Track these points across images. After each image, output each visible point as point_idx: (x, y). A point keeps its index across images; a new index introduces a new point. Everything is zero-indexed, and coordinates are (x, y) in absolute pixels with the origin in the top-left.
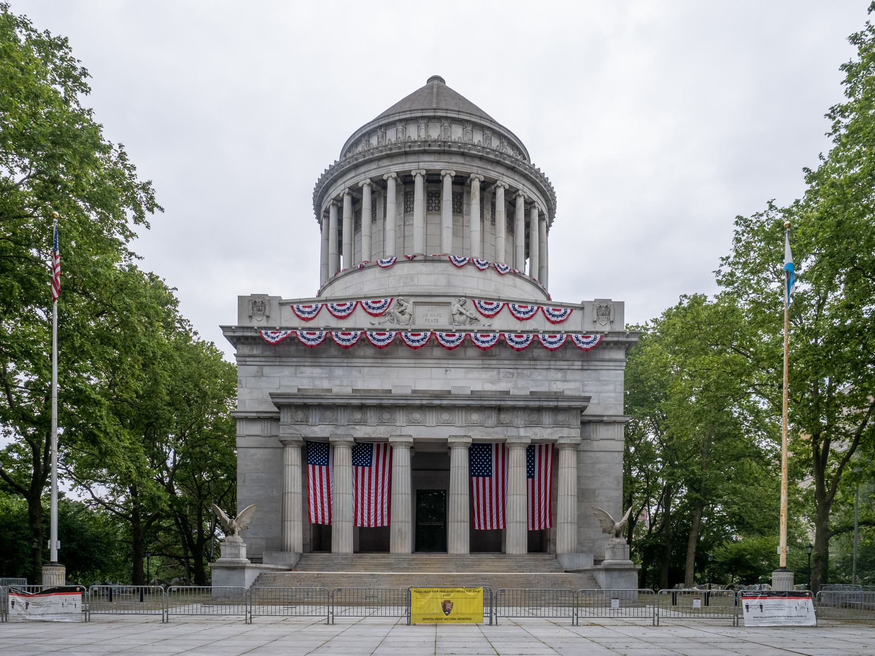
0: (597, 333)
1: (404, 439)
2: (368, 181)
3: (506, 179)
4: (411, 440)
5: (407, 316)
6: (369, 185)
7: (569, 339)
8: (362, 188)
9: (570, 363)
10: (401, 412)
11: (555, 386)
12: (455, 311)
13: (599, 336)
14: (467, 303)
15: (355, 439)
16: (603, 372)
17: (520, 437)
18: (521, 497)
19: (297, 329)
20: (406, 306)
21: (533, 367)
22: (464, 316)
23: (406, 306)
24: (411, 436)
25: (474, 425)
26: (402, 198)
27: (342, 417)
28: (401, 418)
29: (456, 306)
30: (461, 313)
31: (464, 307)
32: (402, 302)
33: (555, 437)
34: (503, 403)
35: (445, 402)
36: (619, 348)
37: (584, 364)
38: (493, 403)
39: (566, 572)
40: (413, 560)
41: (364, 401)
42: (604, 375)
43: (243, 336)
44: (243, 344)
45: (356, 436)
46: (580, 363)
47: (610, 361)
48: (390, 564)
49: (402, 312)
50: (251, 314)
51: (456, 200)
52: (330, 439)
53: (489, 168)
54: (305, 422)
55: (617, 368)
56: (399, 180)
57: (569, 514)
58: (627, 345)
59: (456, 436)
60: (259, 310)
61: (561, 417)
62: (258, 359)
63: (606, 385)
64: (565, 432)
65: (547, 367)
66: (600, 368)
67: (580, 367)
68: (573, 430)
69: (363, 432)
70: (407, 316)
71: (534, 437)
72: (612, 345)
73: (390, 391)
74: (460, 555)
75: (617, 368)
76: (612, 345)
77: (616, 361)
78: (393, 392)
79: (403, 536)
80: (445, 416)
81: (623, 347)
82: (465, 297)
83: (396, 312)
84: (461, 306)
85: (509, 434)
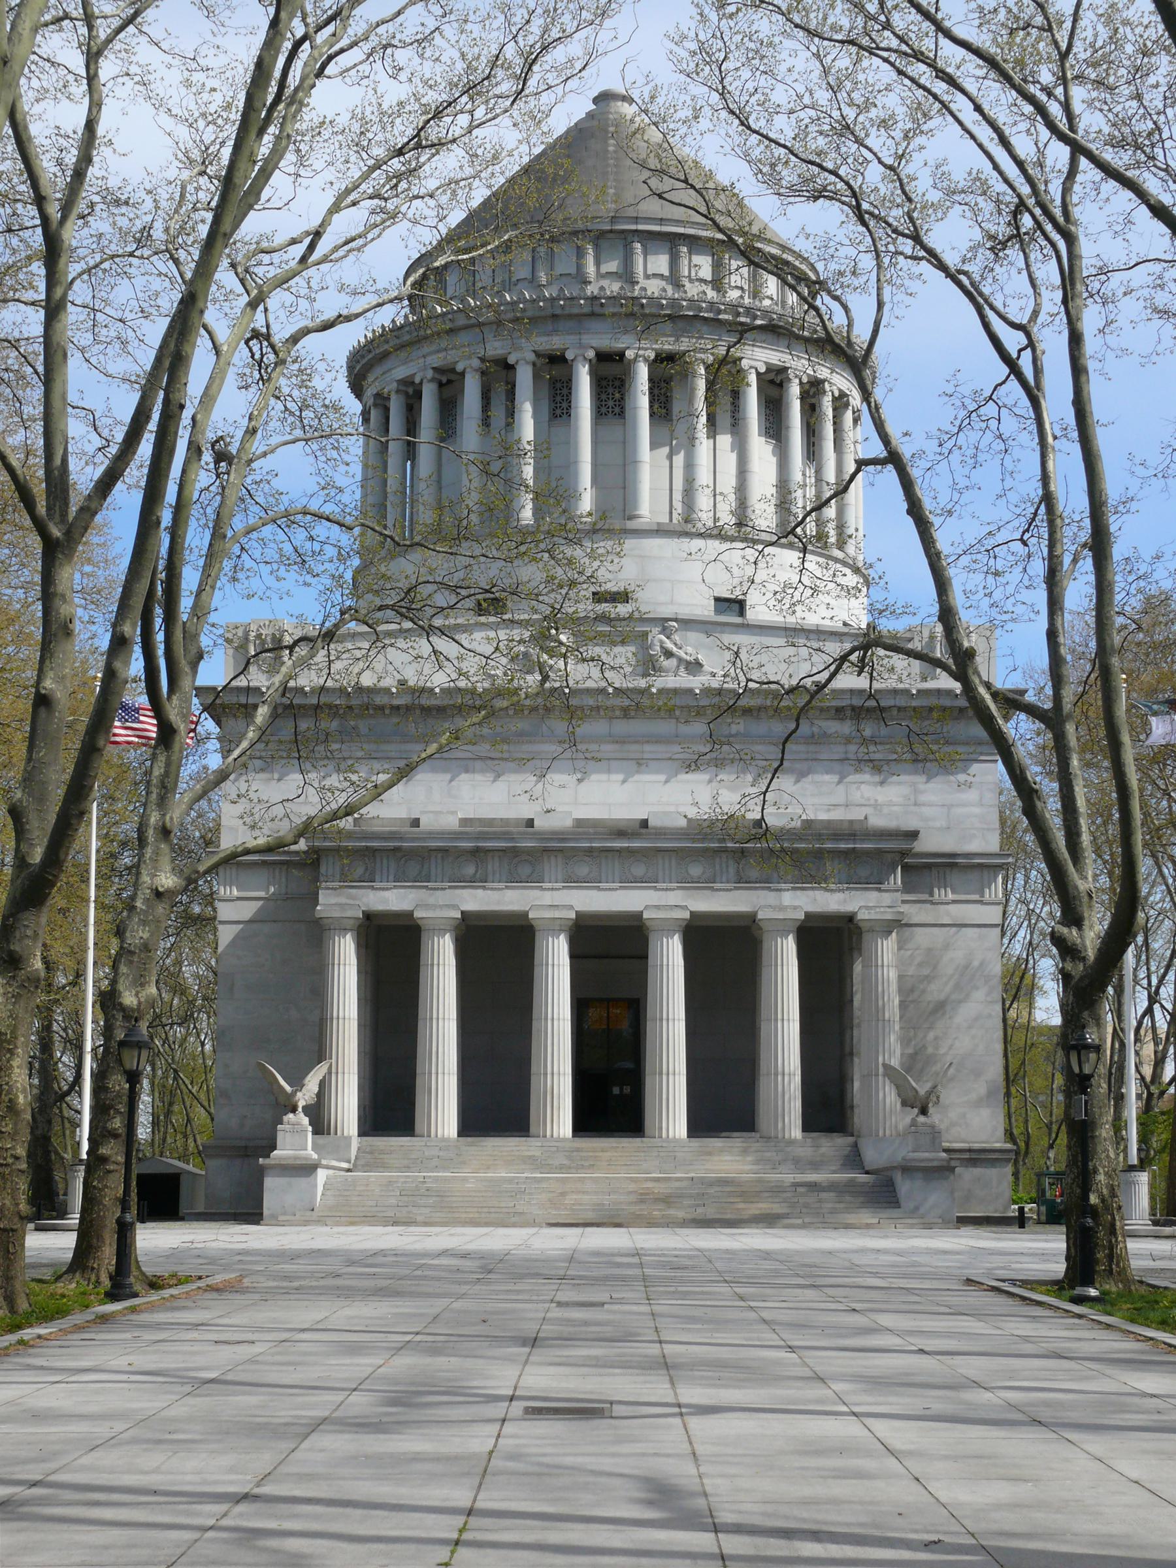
1: (557, 914)
2: (476, 363)
4: (574, 916)
8: (463, 374)
10: (553, 859)
11: (858, 794)
15: (462, 912)
17: (782, 908)
21: (814, 756)
24: (571, 907)
26: (545, 392)
30: (668, 654)
39: (867, 1173)
40: (578, 1150)
48: (532, 1158)
51: (656, 391)
52: (417, 914)
56: (539, 362)
59: (657, 907)
65: (842, 756)
71: (811, 908)
73: (530, 823)
78: (536, 823)
80: (639, 870)
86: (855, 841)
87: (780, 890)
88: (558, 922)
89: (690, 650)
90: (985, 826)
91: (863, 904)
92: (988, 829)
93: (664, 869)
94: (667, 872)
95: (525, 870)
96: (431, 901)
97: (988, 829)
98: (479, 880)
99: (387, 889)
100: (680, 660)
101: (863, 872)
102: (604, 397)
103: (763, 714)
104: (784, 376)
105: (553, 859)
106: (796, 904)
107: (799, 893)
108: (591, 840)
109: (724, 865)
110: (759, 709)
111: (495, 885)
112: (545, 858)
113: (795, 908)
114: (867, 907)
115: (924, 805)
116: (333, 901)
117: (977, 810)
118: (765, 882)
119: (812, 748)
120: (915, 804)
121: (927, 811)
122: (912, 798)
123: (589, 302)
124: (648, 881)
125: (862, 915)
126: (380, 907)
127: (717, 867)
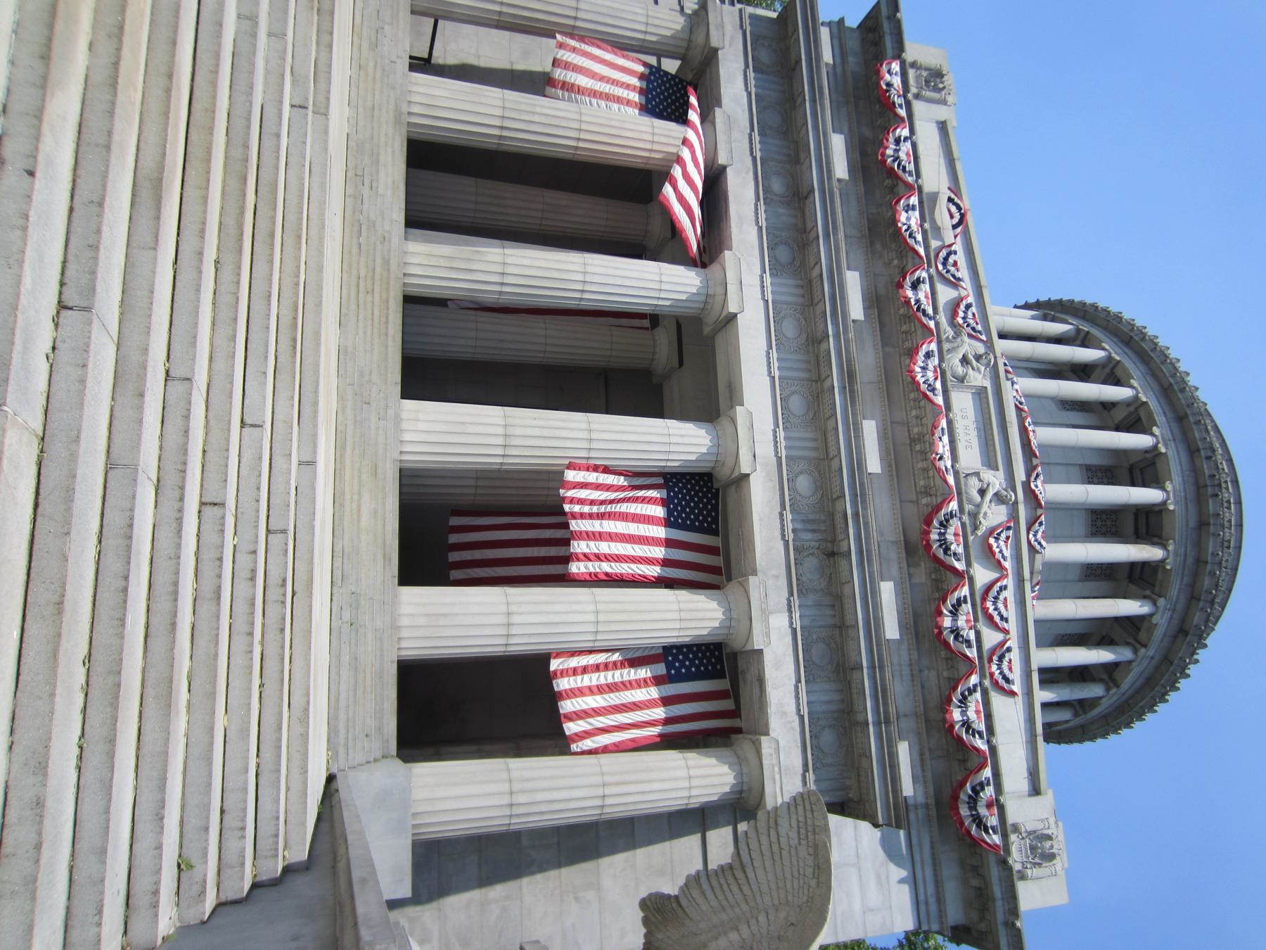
0: (1005, 836)
3: (1168, 615)
5: (960, 370)
6: (1110, 358)
7: (975, 761)
13: (996, 839)
17: (766, 614)
19: (912, 131)
20: (979, 370)
22: (978, 498)
23: (979, 370)
29: (996, 480)
30: (982, 492)
32: (984, 361)
37: (921, 812)
43: (881, 37)
44: (863, 40)
45: (730, 174)
47: (938, 883)
49: (965, 360)
53: (1185, 579)
55: (922, 908)
57: (540, 797)
58: (982, 927)
60: (927, 82)
63: (878, 877)
66: (917, 858)
70: (960, 370)
72: (975, 882)
74: (398, 429)
75: (922, 908)
76: (975, 882)
77: (940, 900)
80: (797, 403)
81: (975, 916)
84: (996, 494)
85: (770, 583)
86: (878, 724)
87: (790, 611)
88: (720, 290)
91: (782, 743)
93: (800, 439)
94: (798, 444)
95: (783, 254)
96: (736, 134)
98: (765, 195)
99: (746, 84)
100: (978, 506)
101: (828, 737)
102: (1099, 474)
104: (1138, 646)
105: (800, 291)
106: (774, 636)
107: (789, 639)
108: (837, 336)
109: (815, 527)
111: (762, 216)
113: (768, 634)
114: (778, 750)
116: (727, 19)
118: (799, 587)
119: (906, 671)
123: (1208, 446)
124: (783, 416)
125: (766, 744)
126: (723, 72)
127: (811, 517)
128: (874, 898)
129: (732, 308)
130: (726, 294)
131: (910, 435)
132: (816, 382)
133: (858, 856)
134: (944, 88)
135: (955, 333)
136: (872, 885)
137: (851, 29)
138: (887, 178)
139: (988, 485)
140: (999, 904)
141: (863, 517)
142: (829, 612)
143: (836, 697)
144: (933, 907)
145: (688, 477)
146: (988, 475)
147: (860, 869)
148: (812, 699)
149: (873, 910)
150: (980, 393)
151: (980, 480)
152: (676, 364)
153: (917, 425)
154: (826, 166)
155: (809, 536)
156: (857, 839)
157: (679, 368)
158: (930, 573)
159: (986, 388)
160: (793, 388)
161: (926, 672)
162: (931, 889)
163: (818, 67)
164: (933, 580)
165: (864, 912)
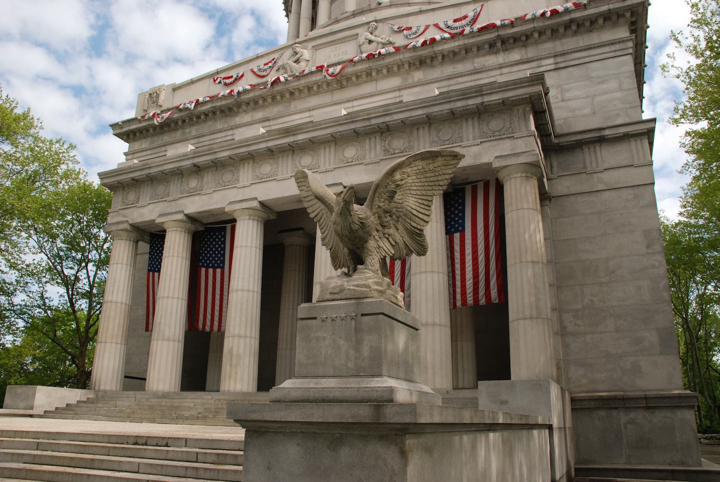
1: (245, 205)
9: (534, 64)
12: (362, 39)
14: (379, 29)
16: (592, 65)
18: (436, 275)
22: (374, 45)
24: (256, 199)
25: (349, 164)
27: (174, 188)
28: (246, 174)
30: (370, 42)
31: (377, 33)
33: (485, 159)
34: (387, 119)
35: (300, 137)
36: (615, 25)
37: (559, 59)
38: (374, 122)
41: (196, 161)
42: (596, 69)
43: (132, 131)
46: (551, 61)
49: (297, 61)
50: (146, 108)
54: (133, 205)
61: (496, 124)
62: (144, 153)
63: (600, 83)
64: (506, 147)
66: (587, 60)
67: (553, 67)
68: (519, 142)
69: (194, 205)
72: (601, 21)
76: (601, 21)
78: (236, 139)
79: (234, 361)
81: (622, 20)
82: (376, 21)
83: (291, 62)
84: (371, 34)
89: (383, 36)
90: (628, 106)
92: (630, 108)
95: (228, 177)
97: (630, 108)
103: (435, 63)
105: (246, 164)
110: (432, 58)
112: (242, 165)
115: (569, 100)
117: (617, 95)
120: (563, 101)
121: (573, 104)
122: (559, 96)
127: (367, 147)
128: (613, 84)
129: (255, 204)
130: (248, 209)
131: (338, 89)
132: (293, 151)
133: (588, 97)
134: (156, 92)
135: (282, 68)
136: (604, 87)
137: (130, 147)
138: (201, 118)
139: (366, 39)
140: (611, 6)
141: (364, 116)
142: (421, 131)
143: (470, 122)
144: (618, 47)
145: (223, 239)
146: (362, 39)
147: (595, 95)
148: (471, 138)
149: (621, 84)
150: (316, 48)
151: (363, 44)
152: (301, 232)
153: (332, 85)
154: (184, 157)
155: (378, 147)
156: (576, 98)
157: (303, 229)
158: (418, 68)
159: (312, 47)
160: (298, 164)
161: (475, 64)
162: (606, 49)
163: (130, 167)
164: (420, 65)
165: (622, 90)
